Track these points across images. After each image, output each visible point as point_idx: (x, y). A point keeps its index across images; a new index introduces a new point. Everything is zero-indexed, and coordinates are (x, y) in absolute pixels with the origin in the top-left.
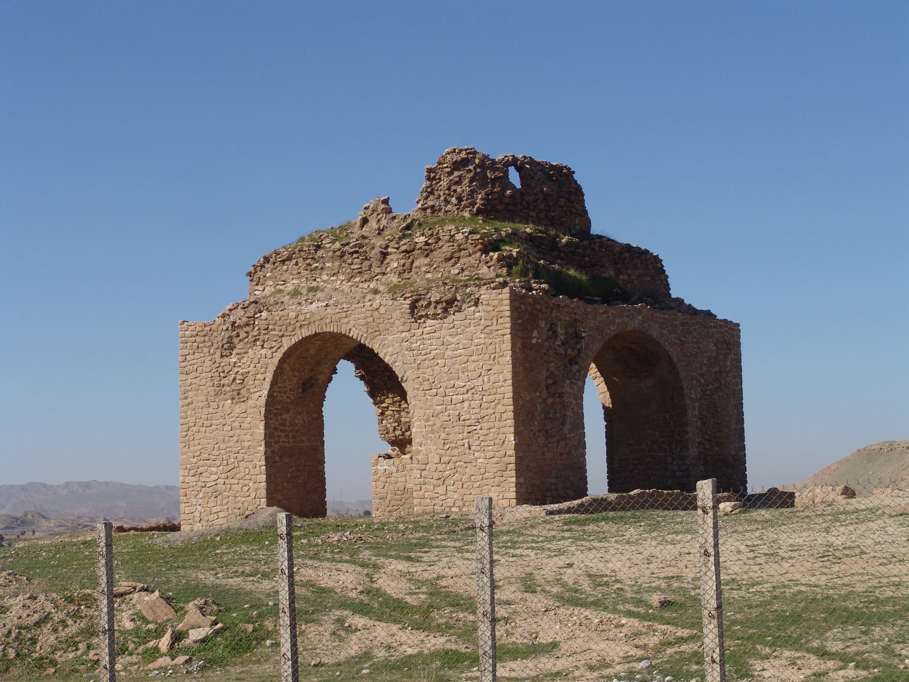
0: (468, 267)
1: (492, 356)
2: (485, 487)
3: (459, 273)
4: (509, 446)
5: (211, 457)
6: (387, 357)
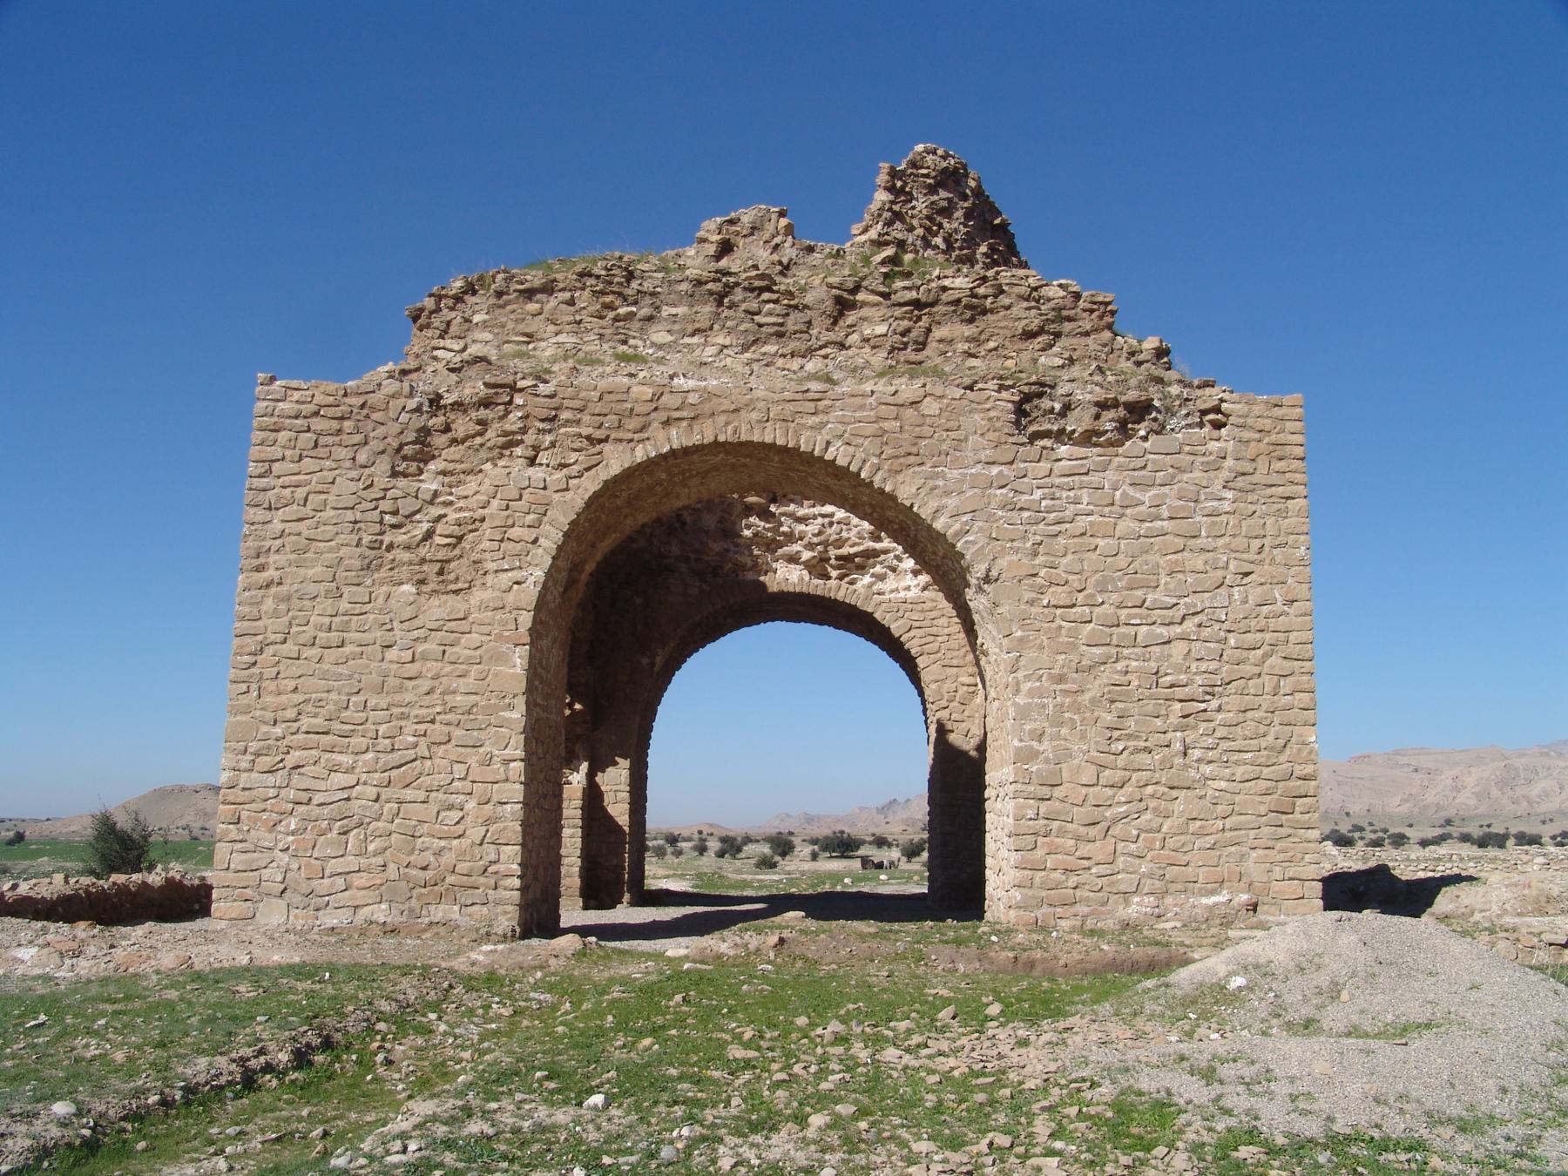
0: (1084, 357)
1: (1256, 544)
2: (1233, 849)
3: (1063, 367)
4: (1304, 753)
5: (336, 726)
6: (942, 519)
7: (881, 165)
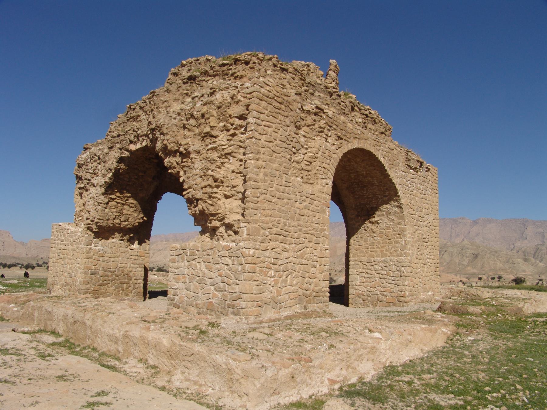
7: (331, 61)
